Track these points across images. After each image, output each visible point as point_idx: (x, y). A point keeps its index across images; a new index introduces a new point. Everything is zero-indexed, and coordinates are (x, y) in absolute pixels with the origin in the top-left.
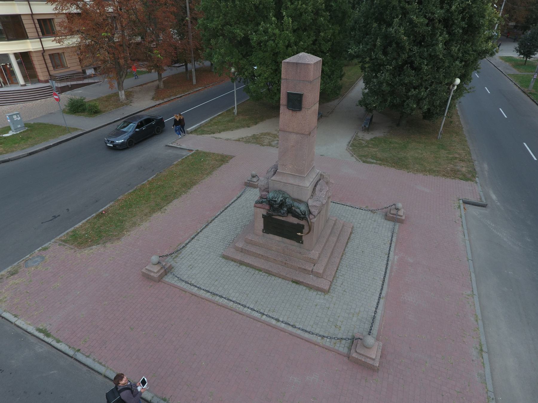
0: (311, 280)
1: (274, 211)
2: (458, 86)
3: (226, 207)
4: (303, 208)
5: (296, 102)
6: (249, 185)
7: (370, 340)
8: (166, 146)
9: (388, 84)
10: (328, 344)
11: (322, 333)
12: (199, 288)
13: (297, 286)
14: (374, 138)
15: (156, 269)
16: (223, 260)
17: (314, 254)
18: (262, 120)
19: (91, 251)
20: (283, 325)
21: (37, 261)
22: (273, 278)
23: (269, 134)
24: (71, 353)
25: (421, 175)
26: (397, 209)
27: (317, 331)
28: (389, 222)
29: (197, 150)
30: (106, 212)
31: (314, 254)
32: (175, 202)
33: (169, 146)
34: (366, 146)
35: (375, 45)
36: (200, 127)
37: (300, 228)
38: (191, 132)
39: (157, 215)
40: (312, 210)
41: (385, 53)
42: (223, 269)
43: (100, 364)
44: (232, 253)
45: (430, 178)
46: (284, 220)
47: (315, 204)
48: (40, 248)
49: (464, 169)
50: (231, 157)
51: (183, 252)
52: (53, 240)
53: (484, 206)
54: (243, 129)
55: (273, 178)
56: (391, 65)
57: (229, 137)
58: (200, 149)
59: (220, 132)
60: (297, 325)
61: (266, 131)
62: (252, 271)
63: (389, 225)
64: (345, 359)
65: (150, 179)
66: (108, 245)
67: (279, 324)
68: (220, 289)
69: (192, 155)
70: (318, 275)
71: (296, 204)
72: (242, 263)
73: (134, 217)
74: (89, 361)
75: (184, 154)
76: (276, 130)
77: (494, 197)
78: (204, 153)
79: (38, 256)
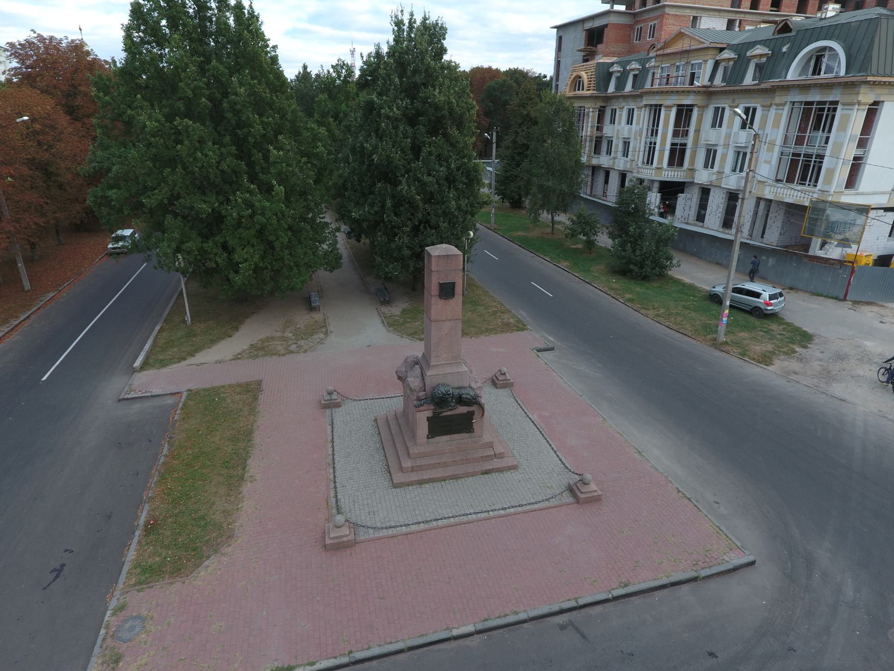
0: (496, 463)
1: (441, 408)
2: (472, 239)
3: (330, 439)
4: (472, 393)
5: (447, 291)
6: (330, 405)
7: (588, 476)
8: (120, 400)
9: (408, 247)
10: (556, 503)
11: (545, 498)
12: (407, 525)
13: (490, 475)
14: (404, 310)
15: (345, 531)
16: (398, 490)
17: (487, 438)
18: (241, 323)
19: (210, 570)
20: (512, 510)
21: (132, 628)
22: (463, 480)
23: (273, 338)
24: (345, 660)
25: (483, 338)
26: (504, 374)
27: (540, 499)
28: (502, 390)
29: (189, 390)
30: (156, 521)
31: (487, 438)
32: (250, 462)
33: (127, 399)
34: (405, 322)
35: (383, 207)
36: (147, 357)
37: (471, 414)
38: (143, 368)
39: (246, 488)
40: (478, 392)
41: (396, 215)
42: (408, 497)
43: (391, 643)
44: (399, 478)
45: (493, 338)
46: (452, 414)
47: (479, 385)
48: (109, 613)
49: (512, 321)
50: (259, 383)
51: (343, 506)
52: (117, 593)
53: (552, 349)
54: (223, 342)
55: (429, 373)
56: (407, 226)
57: (219, 357)
58: (193, 386)
59: (192, 354)
60: (521, 503)
61: (263, 336)
62: (440, 485)
63: (503, 394)
64: (576, 505)
65: (165, 451)
66: (225, 550)
67: (508, 511)
68: (427, 514)
69: (189, 398)
70: (500, 456)
71: (463, 391)
72: (421, 483)
73: (214, 504)
74: (376, 651)
75: (170, 401)
76: (277, 331)
77: (551, 338)
78: (205, 390)
79: (125, 621)
